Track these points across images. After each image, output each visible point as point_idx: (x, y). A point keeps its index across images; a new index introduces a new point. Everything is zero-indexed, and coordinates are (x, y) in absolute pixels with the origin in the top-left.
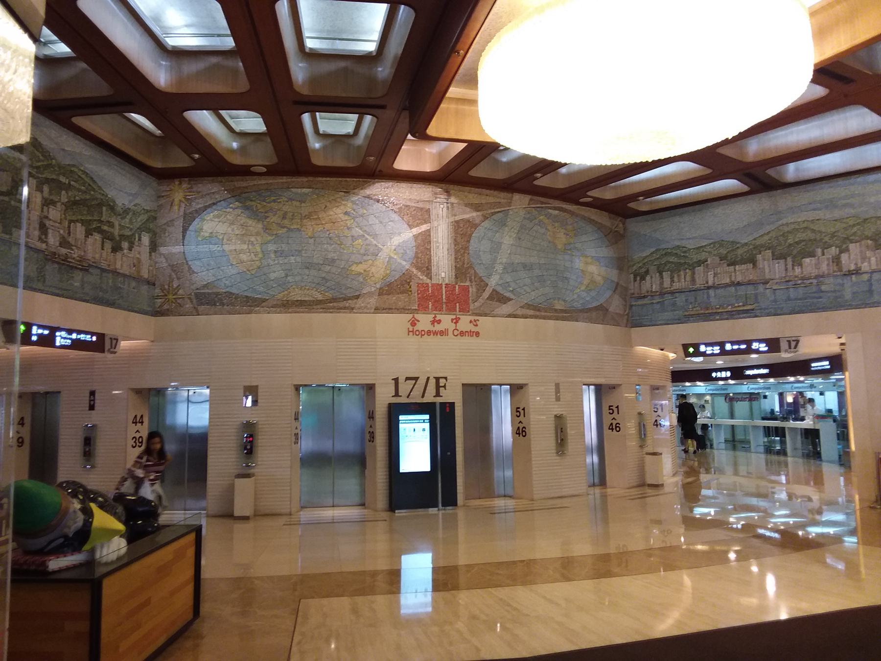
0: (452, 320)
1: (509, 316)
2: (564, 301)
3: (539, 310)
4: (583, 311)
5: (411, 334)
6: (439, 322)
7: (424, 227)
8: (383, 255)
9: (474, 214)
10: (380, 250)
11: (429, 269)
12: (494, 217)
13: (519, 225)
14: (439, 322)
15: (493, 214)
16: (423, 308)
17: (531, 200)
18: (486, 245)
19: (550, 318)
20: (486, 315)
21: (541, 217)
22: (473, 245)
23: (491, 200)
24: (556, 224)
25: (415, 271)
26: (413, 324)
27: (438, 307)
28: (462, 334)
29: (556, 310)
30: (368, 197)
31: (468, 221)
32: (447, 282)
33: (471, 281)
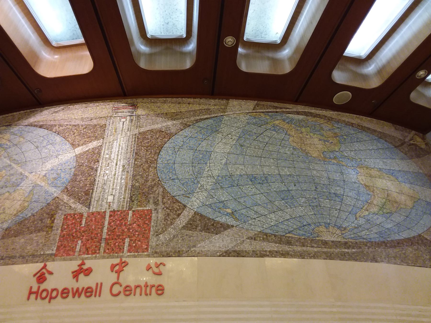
0: (113, 267)
1: (227, 254)
2: (339, 228)
3: (289, 243)
4: (384, 244)
5: (33, 296)
6: (88, 272)
7: (95, 144)
8: (26, 186)
9: (170, 123)
10: (23, 177)
11: (88, 193)
12: (201, 124)
13: (240, 130)
14: (88, 272)
15: (197, 121)
16: (65, 250)
17: (257, 105)
18: (186, 155)
19: (315, 256)
20: (179, 254)
21: (277, 122)
22: (165, 155)
23: (197, 107)
24: (303, 130)
25: (65, 198)
26: (41, 278)
27: (91, 249)
28: (128, 291)
29: (325, 243)
30: (31, 125)
31: (161, 131)
32: (115, 207)
33: (156, 203)
